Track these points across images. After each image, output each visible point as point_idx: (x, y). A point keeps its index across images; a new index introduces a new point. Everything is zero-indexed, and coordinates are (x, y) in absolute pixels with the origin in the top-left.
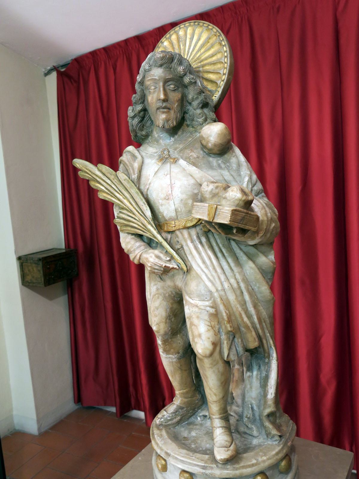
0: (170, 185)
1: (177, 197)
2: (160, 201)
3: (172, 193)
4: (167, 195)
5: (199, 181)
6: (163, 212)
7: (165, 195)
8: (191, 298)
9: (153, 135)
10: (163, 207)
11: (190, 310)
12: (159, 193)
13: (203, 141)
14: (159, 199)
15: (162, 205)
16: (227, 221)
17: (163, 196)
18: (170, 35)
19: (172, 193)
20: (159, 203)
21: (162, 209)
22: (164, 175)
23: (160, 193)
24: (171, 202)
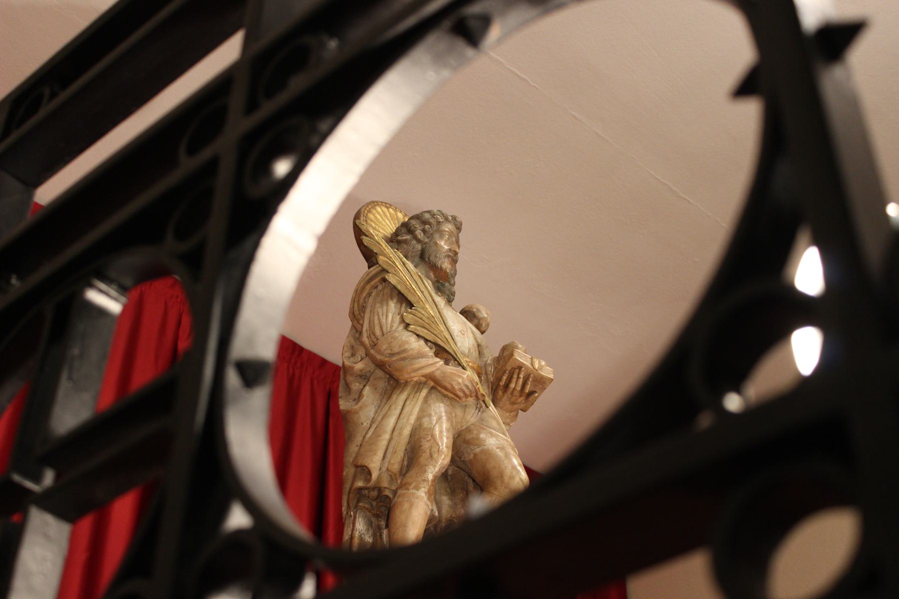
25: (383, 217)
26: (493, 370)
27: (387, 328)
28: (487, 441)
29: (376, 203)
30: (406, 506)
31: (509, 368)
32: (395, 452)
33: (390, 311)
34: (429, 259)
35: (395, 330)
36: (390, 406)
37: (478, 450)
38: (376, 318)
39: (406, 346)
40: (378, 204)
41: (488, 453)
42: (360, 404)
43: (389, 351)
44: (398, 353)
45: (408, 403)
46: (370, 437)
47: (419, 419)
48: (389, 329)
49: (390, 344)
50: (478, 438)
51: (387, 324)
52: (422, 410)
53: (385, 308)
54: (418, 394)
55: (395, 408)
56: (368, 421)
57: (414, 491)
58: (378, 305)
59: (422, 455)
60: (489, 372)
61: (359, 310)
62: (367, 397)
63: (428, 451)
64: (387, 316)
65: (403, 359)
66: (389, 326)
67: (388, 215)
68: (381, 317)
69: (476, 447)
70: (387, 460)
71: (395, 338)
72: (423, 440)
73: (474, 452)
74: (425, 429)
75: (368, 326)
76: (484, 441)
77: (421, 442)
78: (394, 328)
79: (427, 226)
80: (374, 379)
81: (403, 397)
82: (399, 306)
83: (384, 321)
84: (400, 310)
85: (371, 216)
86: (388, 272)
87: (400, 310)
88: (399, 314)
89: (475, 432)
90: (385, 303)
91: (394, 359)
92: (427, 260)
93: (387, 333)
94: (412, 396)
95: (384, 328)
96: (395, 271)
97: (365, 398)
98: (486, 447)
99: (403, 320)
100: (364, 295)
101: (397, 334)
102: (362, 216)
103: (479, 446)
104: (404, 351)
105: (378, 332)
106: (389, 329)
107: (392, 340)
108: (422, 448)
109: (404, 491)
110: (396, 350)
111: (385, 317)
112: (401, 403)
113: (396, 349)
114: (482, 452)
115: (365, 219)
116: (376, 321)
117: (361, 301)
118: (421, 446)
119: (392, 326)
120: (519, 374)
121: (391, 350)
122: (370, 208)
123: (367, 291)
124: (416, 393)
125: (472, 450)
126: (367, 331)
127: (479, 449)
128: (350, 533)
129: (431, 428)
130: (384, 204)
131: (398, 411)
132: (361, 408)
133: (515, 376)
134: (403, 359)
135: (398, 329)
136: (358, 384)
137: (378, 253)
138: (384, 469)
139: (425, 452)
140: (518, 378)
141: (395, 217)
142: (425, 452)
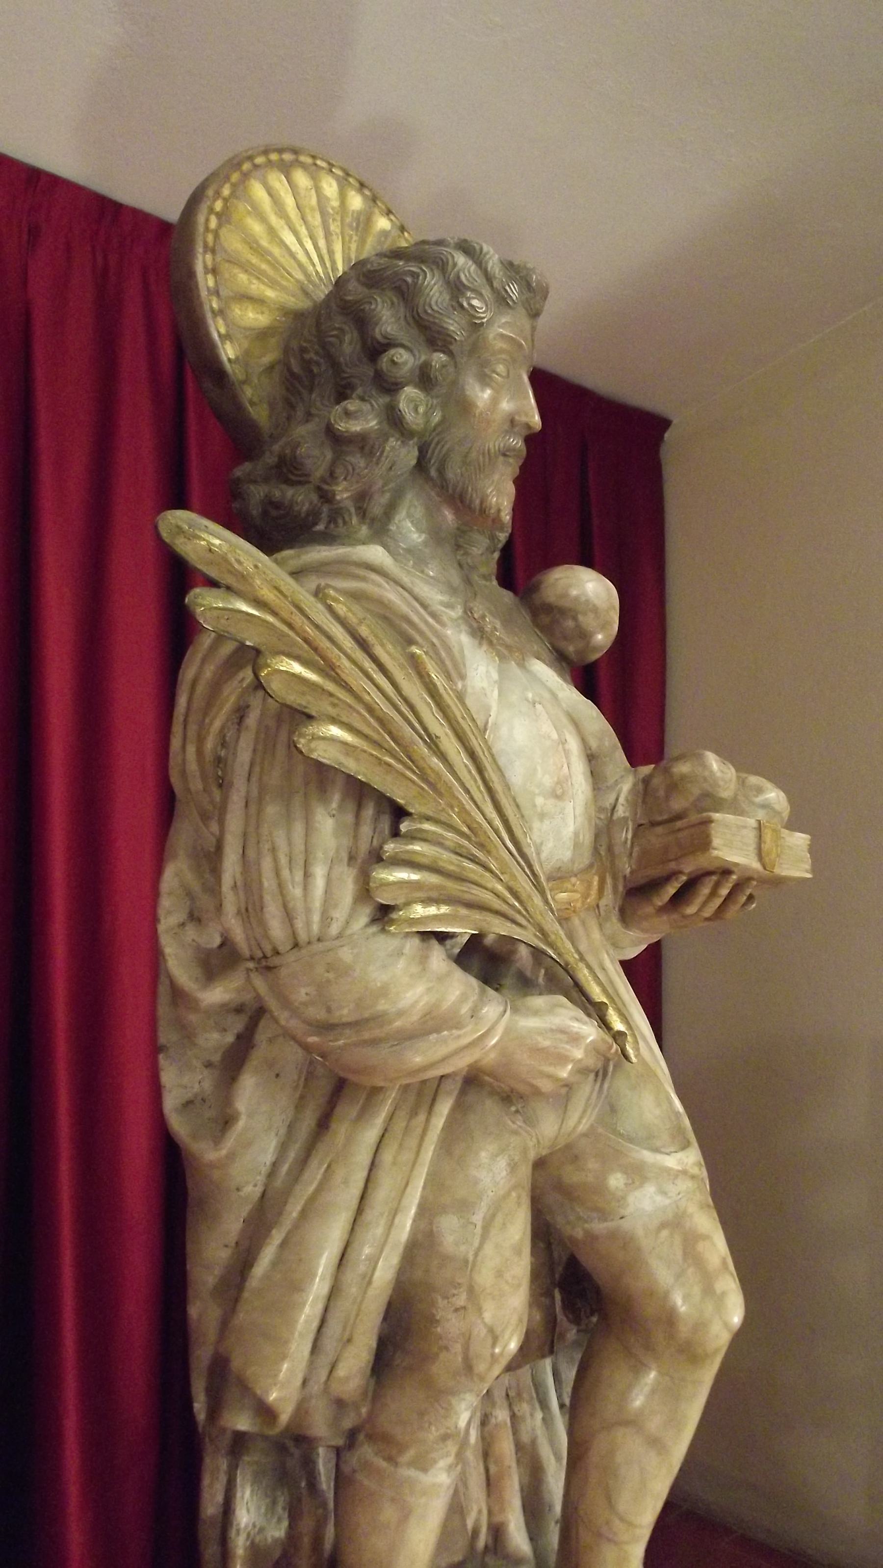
0: (561, 746)
1: (580, 791)
2: (539, 801)
3: (570, 774)
4: (558, 778)
5: (594, 744)
6: (542, 844)
7: (556, 779)
8: (657, 1150)
9: (393, 528)
10: (546, 825)
11: (670, 1194)
12: (535, 770)
13: (591, 616)
14: (537, 791)
15: (542, 816)
16: (807, 871)
17: (548, 781)
18: (282, 160)
19: (570, 774)
20: (535, 806)
21: (540, 830)
22: (527, 700)
23: (539, 768)
24: (569, 807)
25: (274, 220)
26: (630, 836)
27: (308, 924)
28: (631, 1199)
29: (246, 166)
30: (388, 1513)
31: (689, 867)
32: (349, 1341)
33: (320, 855)
34: (441, 471)
35: (340, 936)
36: (329, 1166)
37: (599, 1227)
38: (267, 864)
39: (382, 1006)
40: (256, 166)
41: (626, 1241)
42: (230, 1141)
43: (317, 1013)
44: (356, 1025)
45: (387, 1156)
46: (267, 1277)
47: (426, 1211)
48: (315, 928)
49: (322, 987)
50: (600, 1188)
51: (308, 911)
52: (435, 1182)
53: (299, 828)
54: (422, 1117)
55: (346, 1182)
56: (258, 1178)
57: (412, 1473)
58: (272, 810)
59: (437, 1355)
60: (617, 849)
61: (204, 777)
62: (250, 1116)
63: (458, 1348)
64: (307, 875)
65: (374, 1042)
66: (316, 918)
67: (289, 201)
68: (285, 873)
69: (595, 1215)
70: (324, 1361)
71: (341, 970)
72: (441, 1302)
73: (586, 1226)
74: (446, 1259)
75: (238, 869)
76: (621, 1200)
77: (433, 1304)
78: (334, 930)
79: (439, 358)
80: (270, 1040)
81: (370, 1135)
82: (351, 806)
83: (298, 892)
84: (356, 837)
85: (232, 242)
86: (310, 717)
87: (356, 837)
88: (352, 858)
89: (592, 1165)
90: (297, 800)
91: (341, 1042)
92: (433, 473)
93: (309, 943)
94: (399, 1125)
95: (299, 924)
96: (334, 705)
97: (241, 1124)
98: (625, 1225)
99: (365, 892)
100: (217, 724)
101: (346, 954)
102: (200, 250)
103: (604, 1215)
104: (379, 1019)
105: (277, 930)
106: (315, 928)
107: (331, 976)
108: (439, 1329)
109: (384, 1464)
110: (345, 1013)
111: (299, 876)
112: (362, 1156)
113: (345, 1011)
114: (613, 1235)
115: (209, 263)
116: (268, 883)
117: (210, 744)
118: (432, 1321)
119: (326, 919)
120: (717, 886)
121: (329, 1010)
122: (226, 200)
123: (228, 707)
124: (414, 1113)
125: (579, 1218)
126: (235, 887)
127: (605, 1225)
128: (220, 1498)
129: (466, 1261)
130: (274, 157)
131: (355, 1191)
132: (232, 1156)
133: (705, 890)
134: (374, 1042)
135: (349, 932)
136: (216, 1036)
137: (263, 648)
138: (315, 1388)
139: (446, 1348)
140: (713, 893)
141: (314, 201)
142: (446, 1348)
